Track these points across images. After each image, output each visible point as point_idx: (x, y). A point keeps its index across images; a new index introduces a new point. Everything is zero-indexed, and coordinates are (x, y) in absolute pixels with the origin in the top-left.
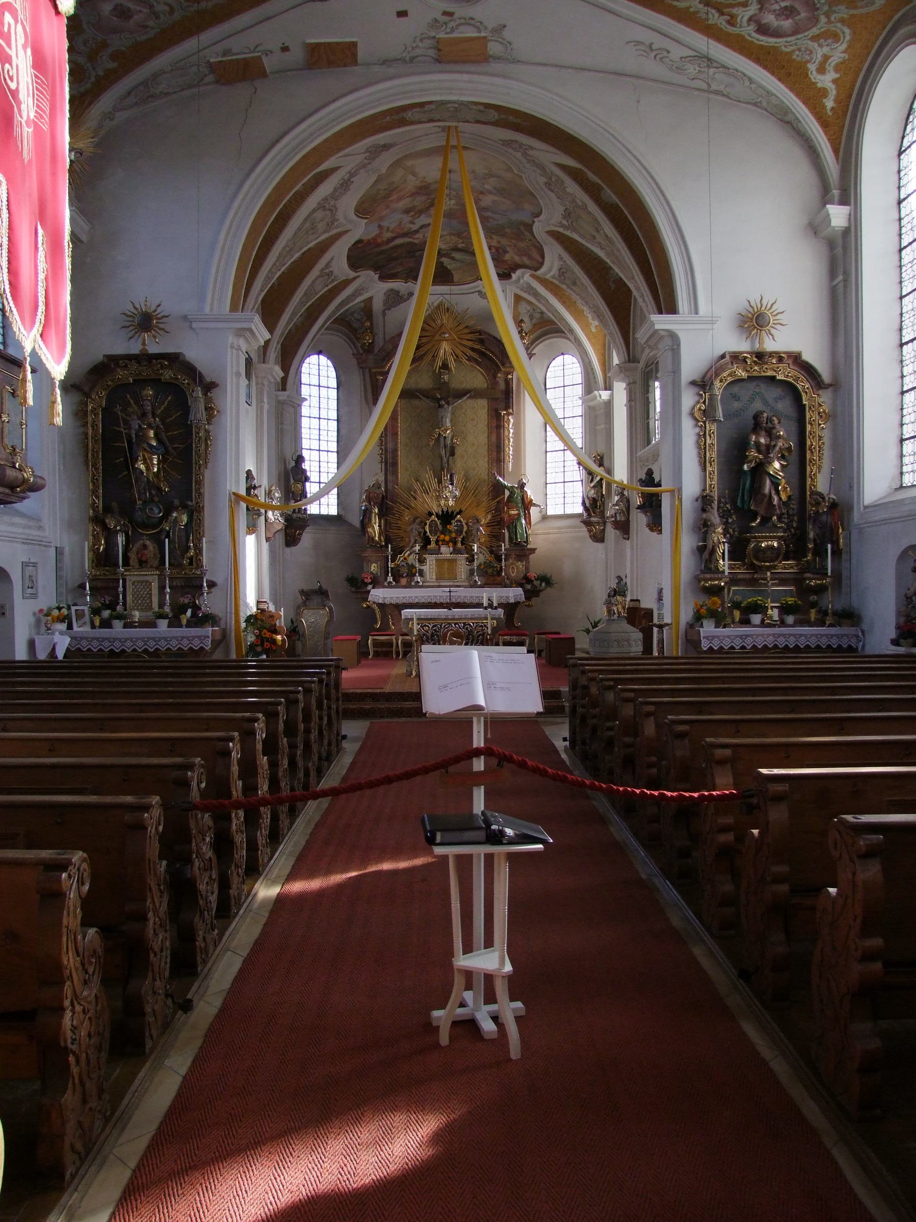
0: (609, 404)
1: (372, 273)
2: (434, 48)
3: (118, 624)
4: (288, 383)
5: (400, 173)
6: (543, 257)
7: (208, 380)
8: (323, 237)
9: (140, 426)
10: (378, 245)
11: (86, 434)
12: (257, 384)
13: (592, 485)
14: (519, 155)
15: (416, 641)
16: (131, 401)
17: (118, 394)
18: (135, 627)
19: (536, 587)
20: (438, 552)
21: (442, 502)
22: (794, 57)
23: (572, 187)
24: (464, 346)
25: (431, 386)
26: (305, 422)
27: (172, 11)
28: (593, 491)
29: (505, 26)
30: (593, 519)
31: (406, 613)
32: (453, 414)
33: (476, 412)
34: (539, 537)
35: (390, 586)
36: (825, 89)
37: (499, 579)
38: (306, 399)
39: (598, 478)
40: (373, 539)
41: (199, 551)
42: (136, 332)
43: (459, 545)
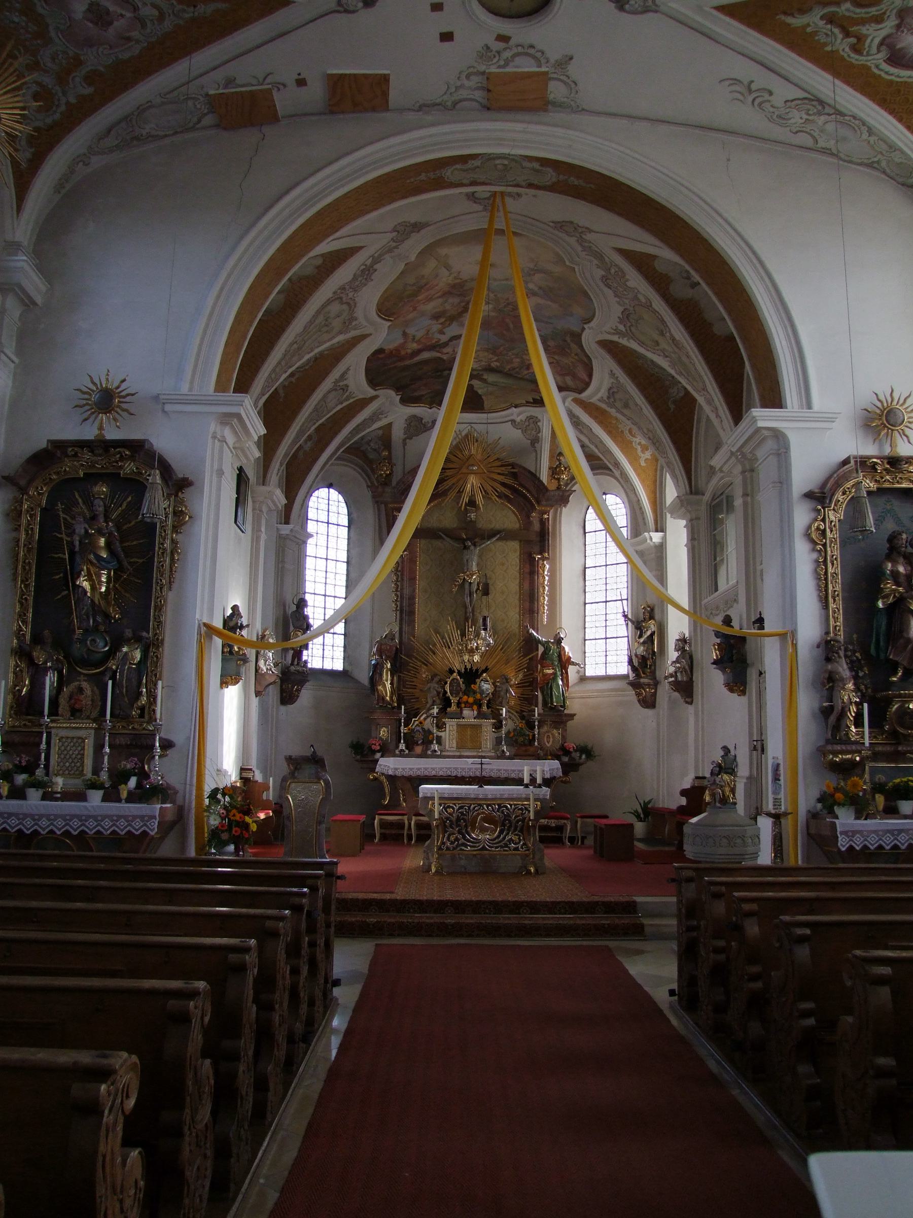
0: (661, 548)
1: (392, 393)
2: (482, 88)
3: (34, 795)
4: (292, 513)
5: (432, 264)
6: (590, 376)
7: (181, 476)
8: (341, 338)
9: (86, 531)
10: (402, 359)
11: (18, 541)
12: (254, 509)
13: (642, 640)
14: (573, 241)
15: (437, 826)
16: (80, 500)
17: (65, 489)
18: (56, 799)
19: (574, 759)
20: (460, 716)
21: (466, 658)
23: (635, 280)
24: (495, 480)
25: (455, 526)
26: (310, 563)
27: (161, 17)
28: (642, 648)
29: (571, 58)
30: (642, 680)
31: (425, 788)
32: (480, 556)
33: (506, 558)
34: (578, 701)
35: (402, 755)
37: (532, 749)
38: (311, 536)
39: (649, 633)
40: (383, 699)
41: (152, 697)
42: (93, 413)
43: (485, 708)
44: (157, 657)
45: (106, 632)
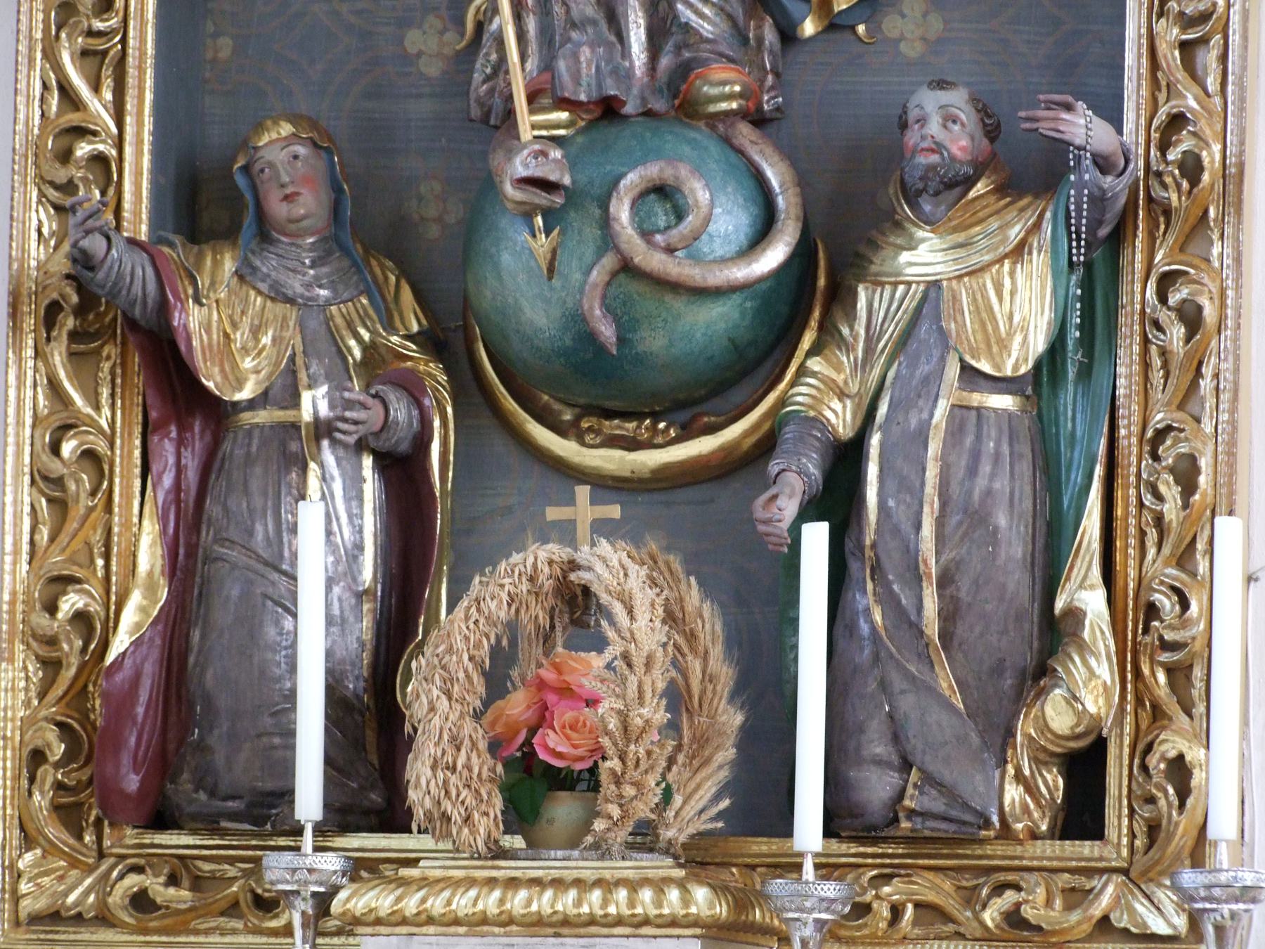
41: (1166, 669)
44: (1192, 318)
45: (759, 120)
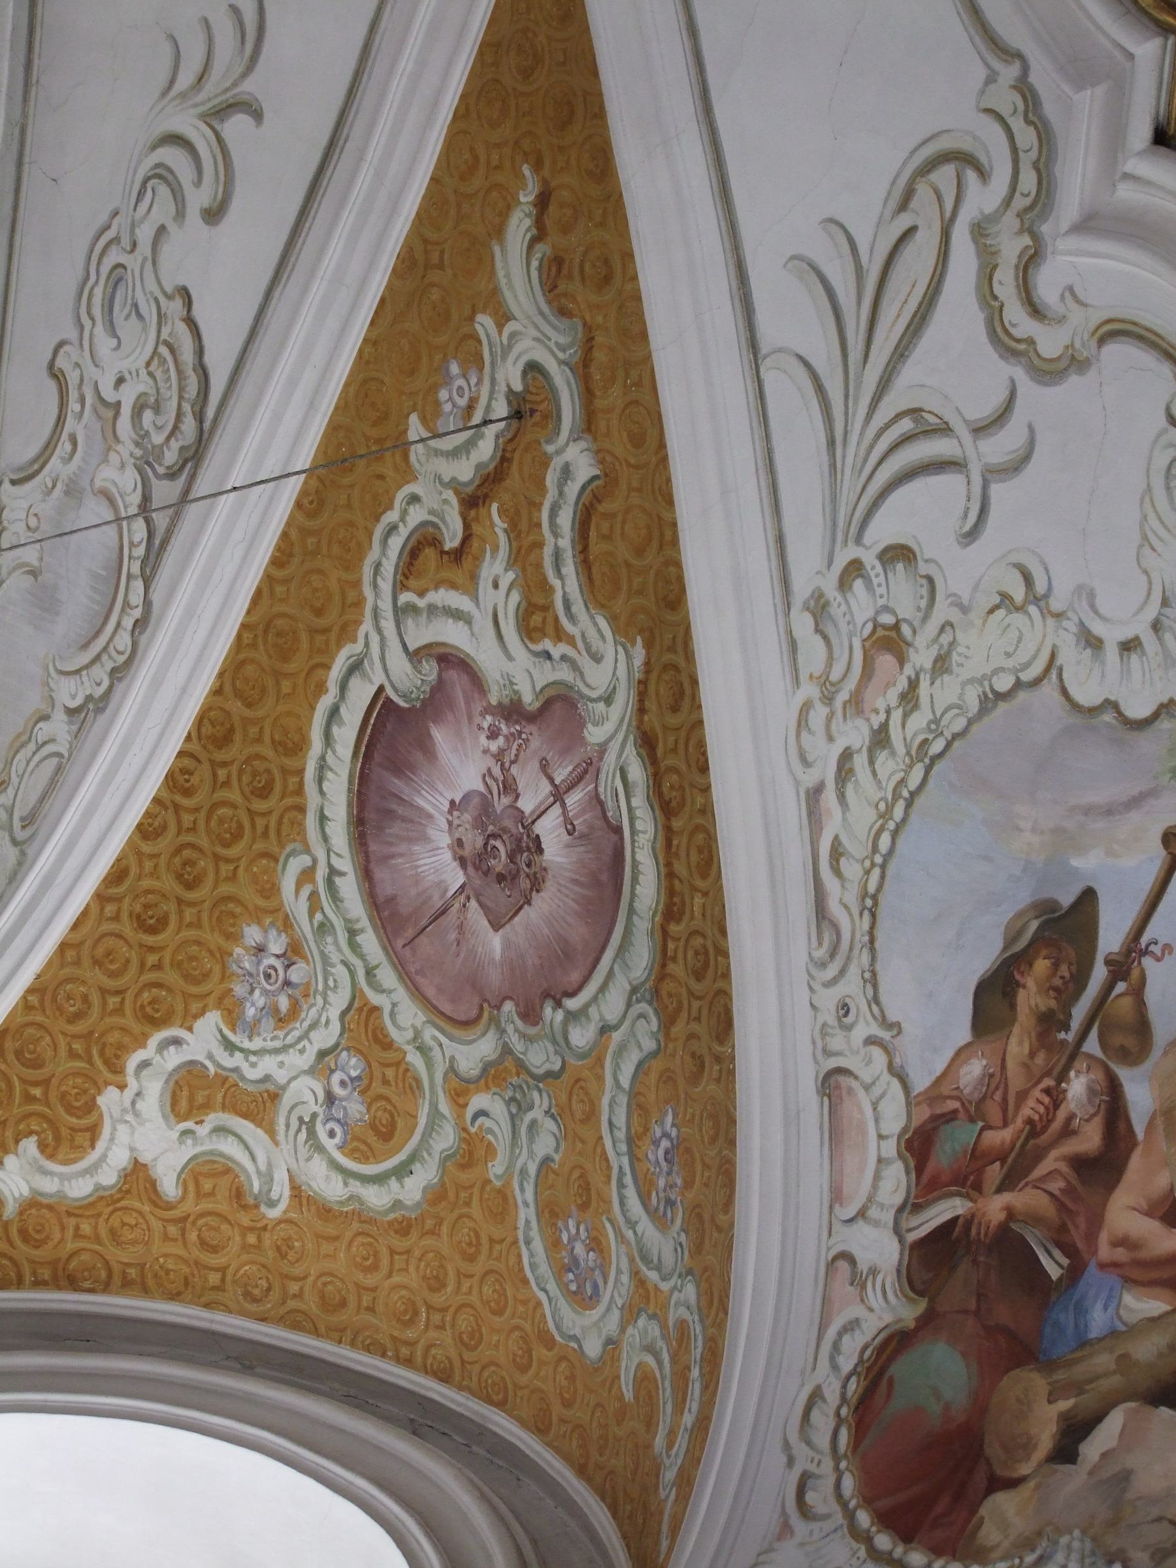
22: (253, 934)
36: (94, 1132)
